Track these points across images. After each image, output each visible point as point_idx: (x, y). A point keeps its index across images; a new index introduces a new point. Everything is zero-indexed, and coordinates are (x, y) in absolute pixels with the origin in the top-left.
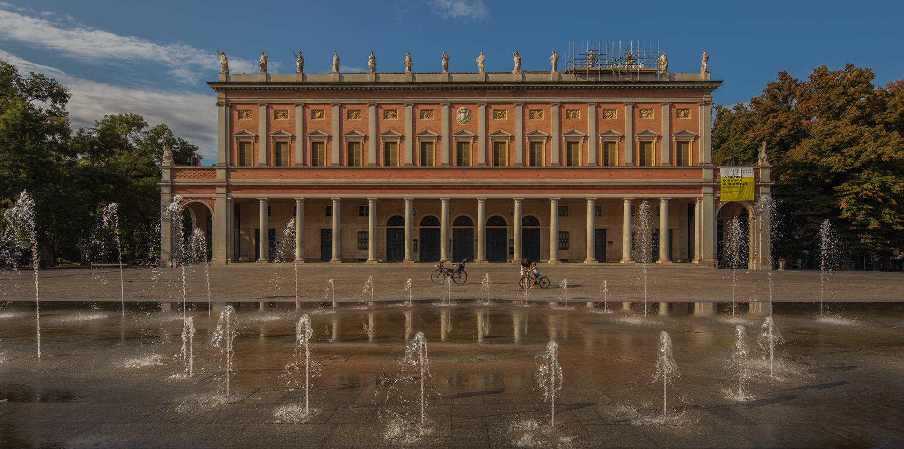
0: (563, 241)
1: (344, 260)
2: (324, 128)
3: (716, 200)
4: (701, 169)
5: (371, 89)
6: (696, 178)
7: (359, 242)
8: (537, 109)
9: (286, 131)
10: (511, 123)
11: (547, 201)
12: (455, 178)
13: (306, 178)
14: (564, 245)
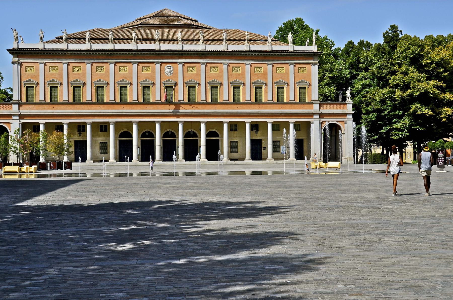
0: (233, 147)
1: (94, 161)
2: (81, 78)
3: (321, 122)
4: (313, 104)
5: (111, 54)
6: (310, 109)
7: (100, 149)
8: (215, 66)
9: (57, 79)
10: (198, 75)
11: (222, 123)
12: (164, 109)
13: (70, 109)
14: (235, 150)
